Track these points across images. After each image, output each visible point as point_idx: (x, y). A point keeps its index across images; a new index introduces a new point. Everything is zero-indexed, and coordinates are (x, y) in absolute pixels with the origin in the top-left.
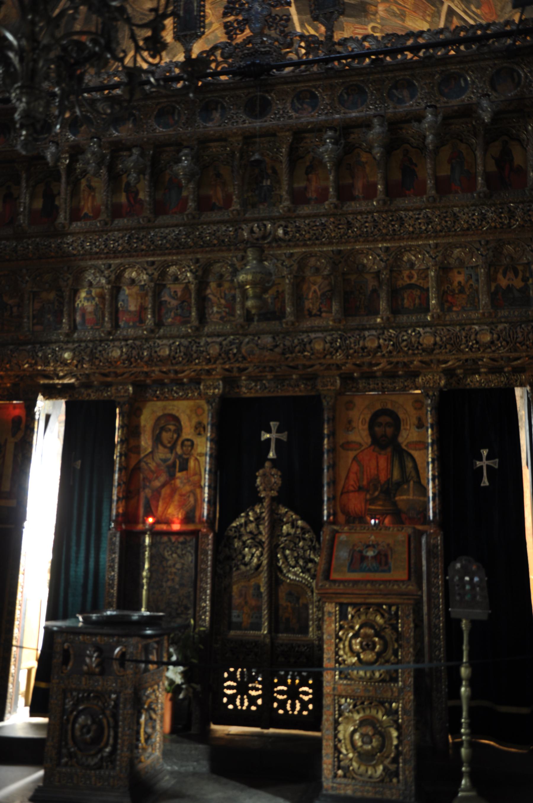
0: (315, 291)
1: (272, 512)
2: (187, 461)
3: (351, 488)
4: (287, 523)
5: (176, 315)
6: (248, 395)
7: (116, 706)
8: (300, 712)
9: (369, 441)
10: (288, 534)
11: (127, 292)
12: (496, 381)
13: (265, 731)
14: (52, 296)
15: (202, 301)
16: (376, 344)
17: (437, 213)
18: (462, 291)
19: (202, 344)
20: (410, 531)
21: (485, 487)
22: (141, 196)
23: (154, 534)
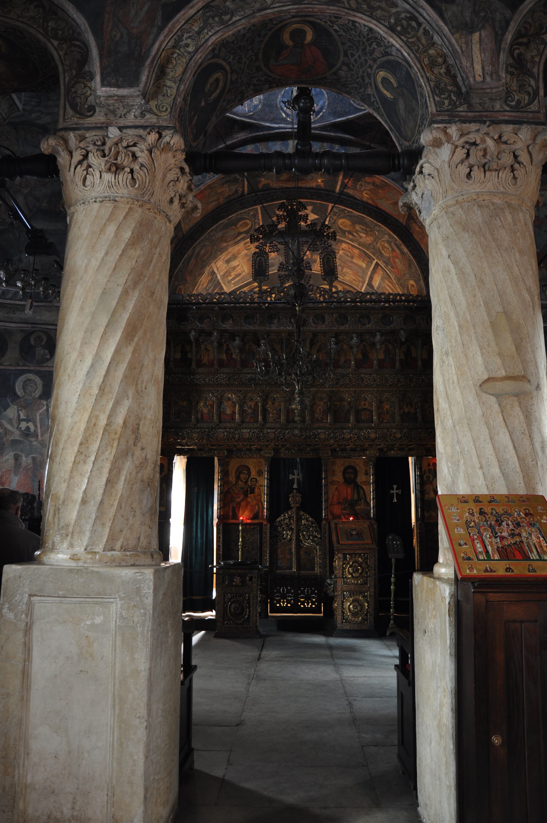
0: (320, 409)
1: (297, 514)
2: (254, 488)
3: (335, 503)
4: (304, 519)
5: (251, 417)
6: (284, 457)
7: (249, 599)
8: (311, 606)
9: (343, 480)
10: (305, 524)
11: (225, 404)
12: (401, 454)
13: (295, 615)
14: (185, 404)
15: (265, 411)
16: (349, 437)
17: (379, 377)
18: (388, 413)
19: (265, 432)
20: (368, 523)
21: (395, 502)
22: (234, 356)
23: (243, 524)
